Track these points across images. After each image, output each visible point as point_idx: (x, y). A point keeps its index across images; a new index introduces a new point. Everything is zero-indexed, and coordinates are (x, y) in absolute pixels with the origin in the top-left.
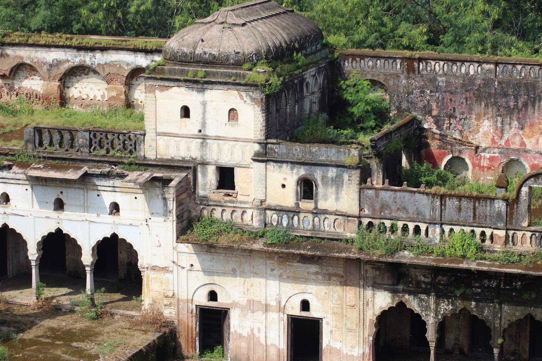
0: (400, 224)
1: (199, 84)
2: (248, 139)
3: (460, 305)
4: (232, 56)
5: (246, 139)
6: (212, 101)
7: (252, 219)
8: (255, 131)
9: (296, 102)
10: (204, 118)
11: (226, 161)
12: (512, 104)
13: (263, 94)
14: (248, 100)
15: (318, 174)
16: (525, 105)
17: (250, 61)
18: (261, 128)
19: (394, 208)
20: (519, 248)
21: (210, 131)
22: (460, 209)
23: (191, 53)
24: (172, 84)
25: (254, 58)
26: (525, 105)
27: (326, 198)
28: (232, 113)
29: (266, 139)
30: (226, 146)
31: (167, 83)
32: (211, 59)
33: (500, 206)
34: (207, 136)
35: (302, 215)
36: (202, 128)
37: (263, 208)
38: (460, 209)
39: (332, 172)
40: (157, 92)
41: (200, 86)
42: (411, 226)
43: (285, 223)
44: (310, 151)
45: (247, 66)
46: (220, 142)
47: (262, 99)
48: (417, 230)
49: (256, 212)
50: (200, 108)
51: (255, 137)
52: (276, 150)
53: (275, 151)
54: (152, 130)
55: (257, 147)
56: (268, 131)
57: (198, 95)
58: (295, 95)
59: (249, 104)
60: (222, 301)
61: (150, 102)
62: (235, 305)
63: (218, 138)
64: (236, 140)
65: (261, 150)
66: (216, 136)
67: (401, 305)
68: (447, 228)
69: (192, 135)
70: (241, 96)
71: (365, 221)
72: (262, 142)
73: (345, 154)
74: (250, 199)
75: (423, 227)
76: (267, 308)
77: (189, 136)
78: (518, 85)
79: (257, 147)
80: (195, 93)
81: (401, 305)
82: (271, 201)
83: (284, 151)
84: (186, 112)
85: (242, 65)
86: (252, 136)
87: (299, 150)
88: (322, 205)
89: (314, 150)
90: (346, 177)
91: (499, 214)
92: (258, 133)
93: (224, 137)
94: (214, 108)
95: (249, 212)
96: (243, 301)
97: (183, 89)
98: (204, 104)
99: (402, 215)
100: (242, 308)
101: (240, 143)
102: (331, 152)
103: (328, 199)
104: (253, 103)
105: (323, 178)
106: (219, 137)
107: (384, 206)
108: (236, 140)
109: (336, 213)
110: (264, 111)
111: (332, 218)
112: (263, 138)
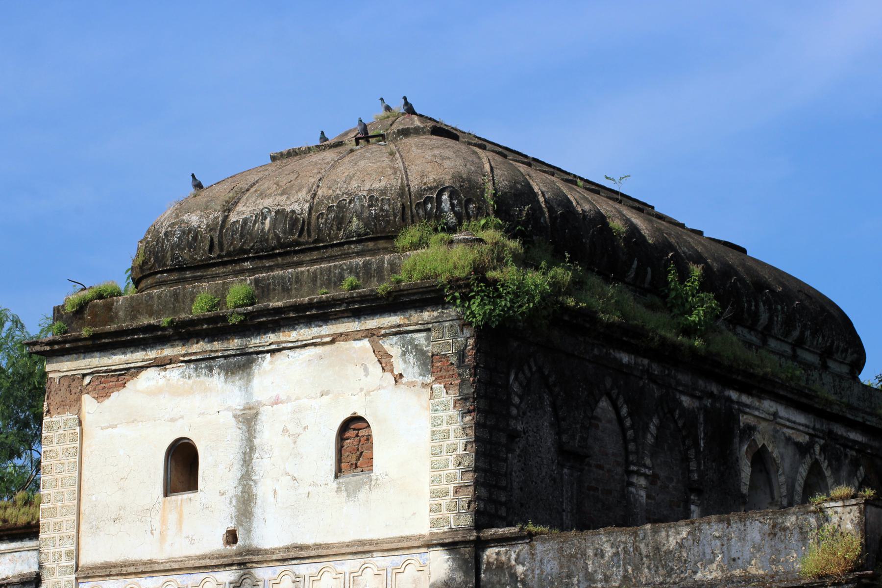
1: (230, 335)
2: (408, 538)
4: (356, 206)
5: (401, 539)
6: (277, 402)
8: (434, 494)
9: (692, 490)
10: (247, 479)
13: (467, 332)
14: (408, 367)
17: (428, 216)
18: (458, 481)
21: (268, 534)
23: (211, 228)
24: (137, 357)
25: (446, 205)
28: (353, 442)
29: (478, 525)
31: (117, 360)
32: (279, 232)
34: (257, 552)
36: (239, 522)
40: (87, 399)
41: (235, 343)
44: (657, 549)
45: (412, 234)
46: (304, 569)
47: (461, 355)
50: (234, 434)
51: (433, 524)
52: (520, 569)
53: (513, 576)
54: (64, 562)
56: (490, 500)
57: (230, 386)
58: (686, 459)
59: (412, 384)
61: (59, 448)
63: (296, 554)
64: (363, 549)
65: (459, 577)
66: (288, 549)
69: (204, 557)
70: (384, 360)
72: (459, 538)
73: (804, 539)
77: (191, 564)
80: (217, 381)
83: (552, 567)
84: (183, 464)
85: (391, 238)
86: (422, 527)
87: (609, 551)
89: (672, 542)
92: (445, 502)
93: (317, 546)
94: (285, 430)
97: (174, 374)
98: (249, 419)
101: (379, 561)
102: (742, 539)
104: (429, 379)
106: (302, 548)
110: (469, 405)
112: (466, 521)
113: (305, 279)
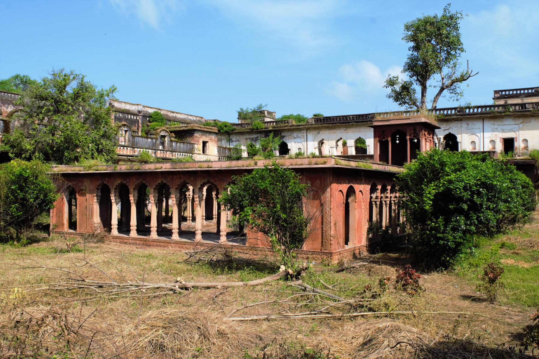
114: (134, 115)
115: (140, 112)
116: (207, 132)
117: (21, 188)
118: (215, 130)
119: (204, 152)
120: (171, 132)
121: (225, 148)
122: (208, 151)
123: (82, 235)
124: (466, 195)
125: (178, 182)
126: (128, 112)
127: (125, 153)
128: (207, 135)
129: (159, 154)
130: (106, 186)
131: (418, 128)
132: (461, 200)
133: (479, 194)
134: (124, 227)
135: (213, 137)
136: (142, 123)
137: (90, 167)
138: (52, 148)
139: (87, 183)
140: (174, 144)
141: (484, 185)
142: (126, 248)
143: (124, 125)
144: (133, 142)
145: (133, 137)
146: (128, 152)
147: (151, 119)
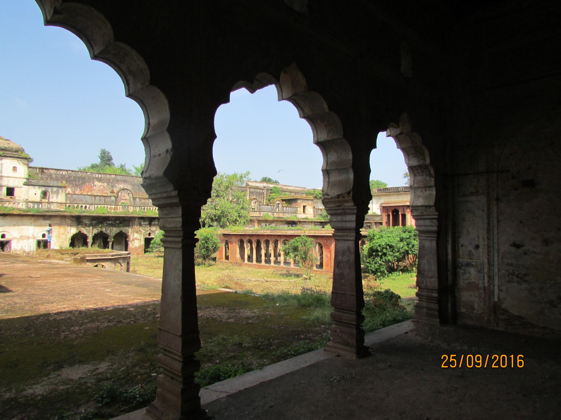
0: (80, 205)
3: (100, 230)
7: (22, 206)
11: (11, 185)
12: (77, 184)
14: (22, 164)
15: (50, 190)
16: (82, 184)
19: (78, 200)
20: (118, 211)
22: (100, 200)
26: (82, 184)
27: (53, 198)
28: (15, 169)
30: (11, 180)
33: (113, 198)
35: (43, 204)
37: (27, 202)
38: (100, 200)
39: (55, 189)
42: (84, 206)
43: (36, 207)
48: (86, 207)
49: (24, 204)
55: (25, 180)
60: (8, 237)
62: (14, 238)
63: (7, 177)
64: (16, 178)
67: (80, 232)
68: (96, 206)
71: (68, 205)
74: (22, 199)
75: (88, 206)
76: (29, 238)
78: (79, 178)
79: (25, 180)
81: (80, 232)
82: (30, 200)
86: (23, 177)
88: (51, 200)
90: (60, 191)
91: (113, 201)
95: (21, 204)
96: (18, 236)
99: (80, 202)
100: (18, 239)
103: (53, 198)
105: (52, 191)
107: (74, 200)
108: (16, 178)
109: (57, 203)
111: (55, 204)
113: (9, 154)
114: (261, 189)
115: (265, 187)
116: (306, 200)
117: (206, 242)
118: (311, 197)
119: (304, 212)
120: (283, 200)
121: (318, 209)
122: (306, 212)
123: (231, 263)
124: (379, 249)
125: (274, 239)
126: (257, 188)
127: (255, 215)
128: (306, 201)
129: (276, 215)
130: (242, 239)
131: (405, 208)
132: (377, 251)
133: (386, 249)
134: (250, 258)
135: (310, 202)
136: (266, 194)
137: (235, 231)
138: (215, 216)
139: (233, 239)
140: (285, 208)
141: (388, 245)
142: (250, 269)
143: (254, 199)
144: (260, 209)
145: (260, 205)
146: (257, 214)
147: (272, 192)
